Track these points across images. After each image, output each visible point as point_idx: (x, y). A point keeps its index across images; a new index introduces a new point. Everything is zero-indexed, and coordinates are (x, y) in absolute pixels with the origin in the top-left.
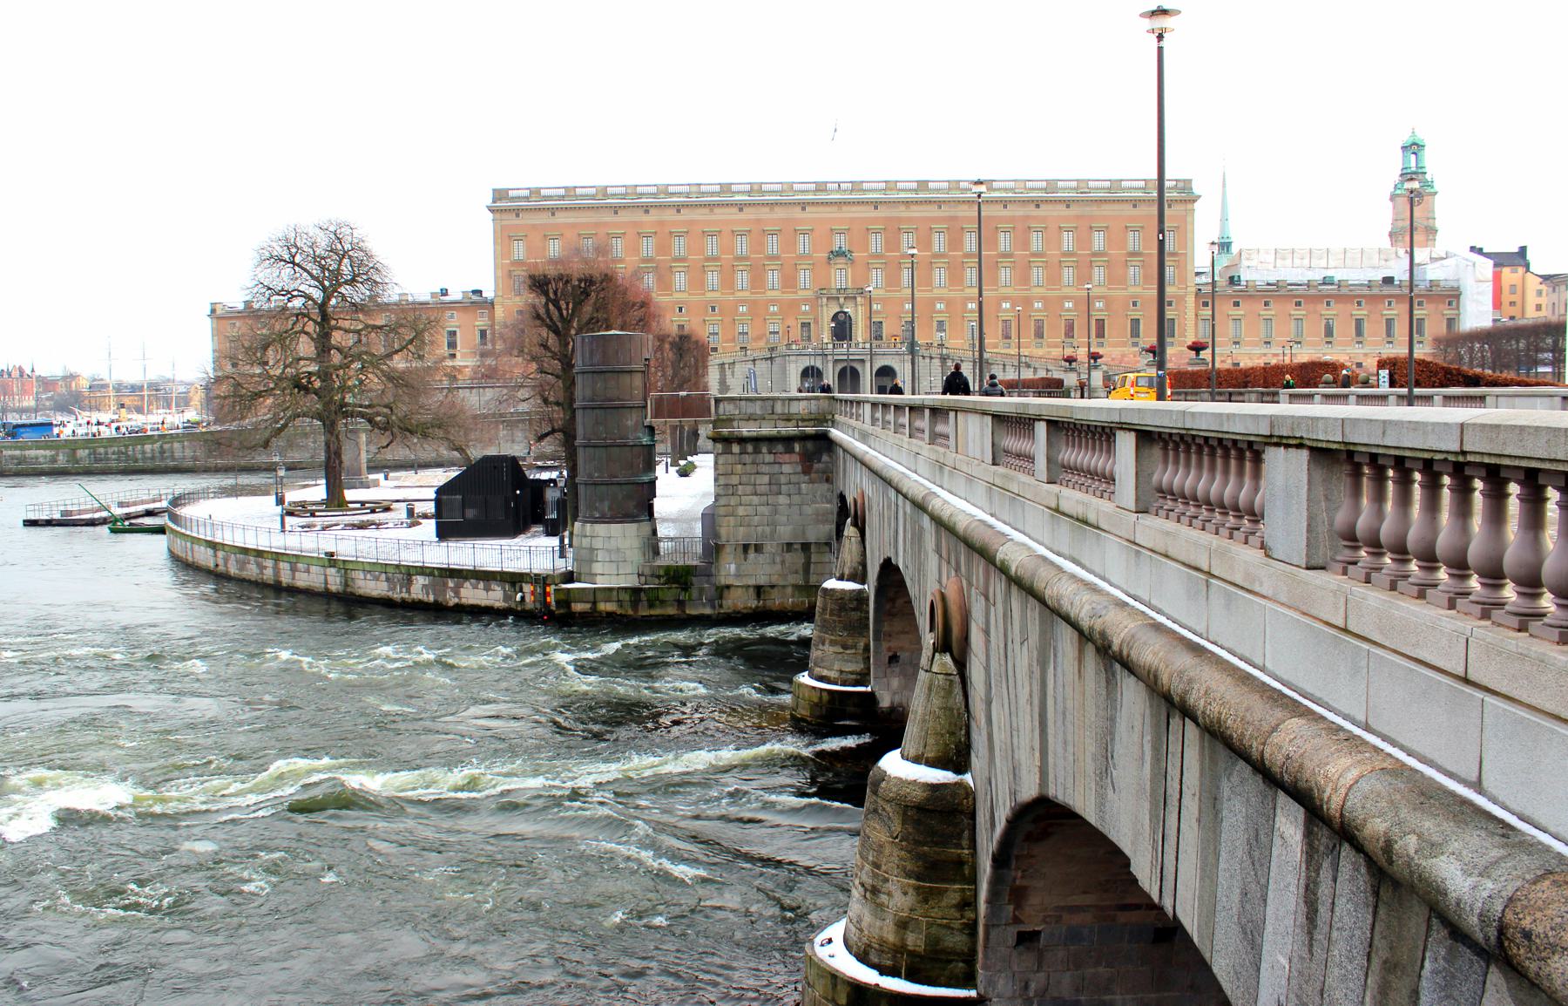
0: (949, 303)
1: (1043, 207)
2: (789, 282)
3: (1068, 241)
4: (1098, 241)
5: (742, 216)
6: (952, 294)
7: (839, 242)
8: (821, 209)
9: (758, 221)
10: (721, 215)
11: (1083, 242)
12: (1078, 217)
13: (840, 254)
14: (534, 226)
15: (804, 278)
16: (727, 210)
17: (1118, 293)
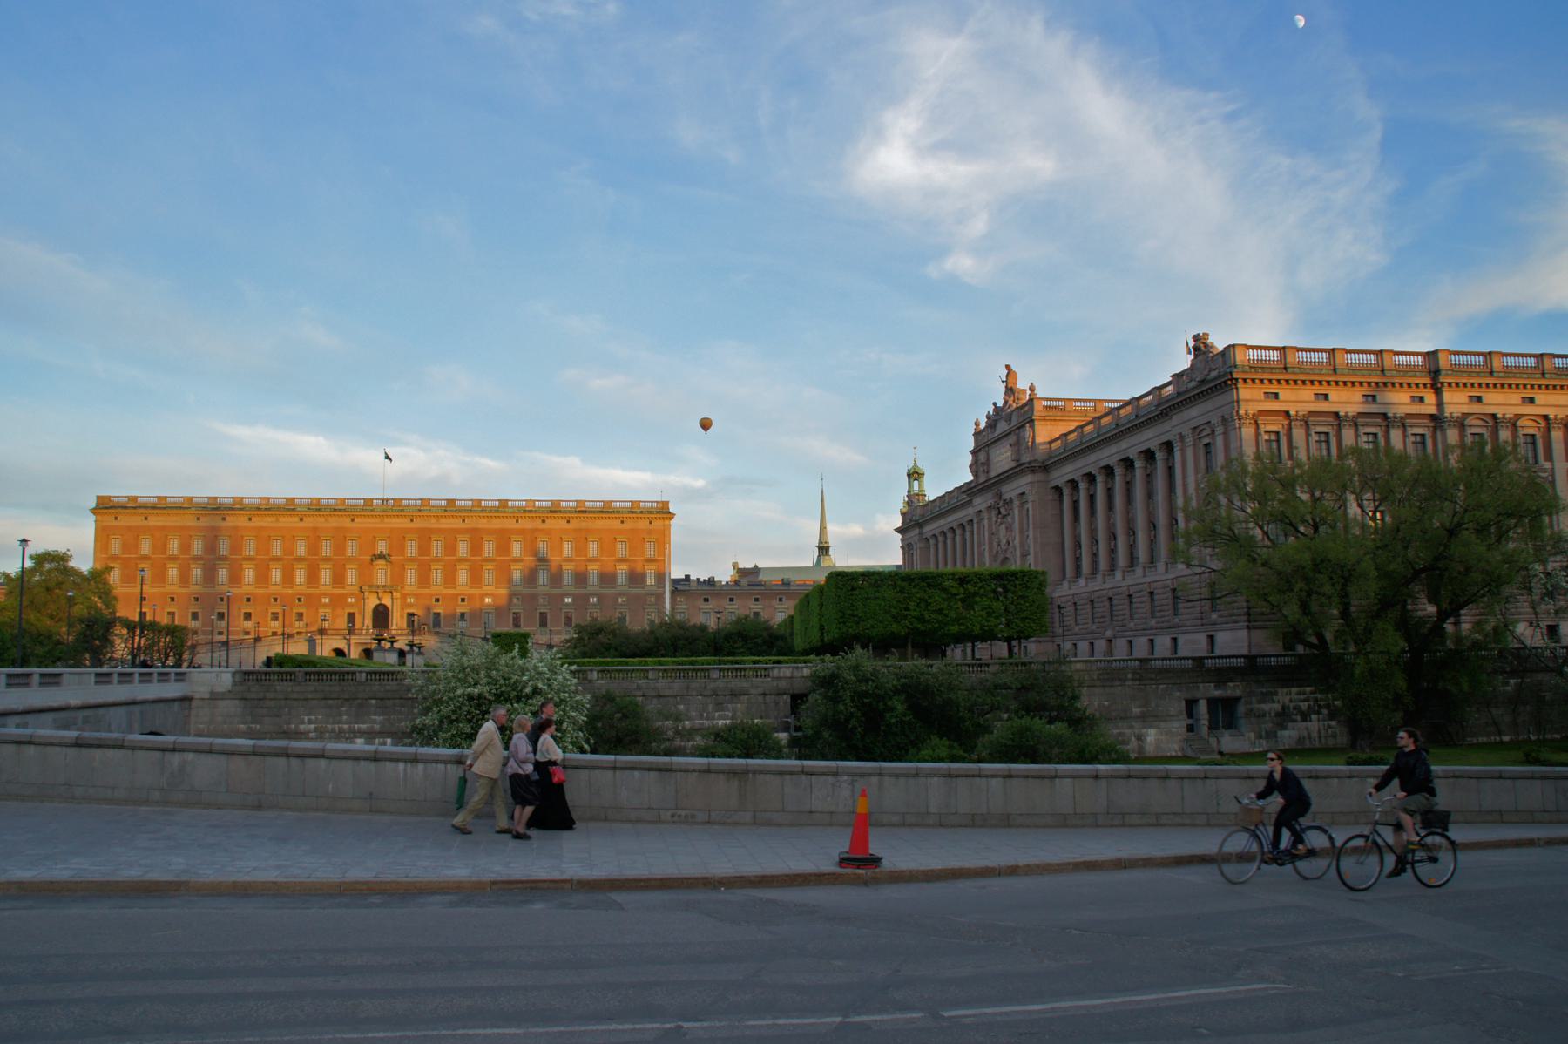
7: (382, 547)
12: (575, 530)
13: (381, 557)
15: (352, 576)
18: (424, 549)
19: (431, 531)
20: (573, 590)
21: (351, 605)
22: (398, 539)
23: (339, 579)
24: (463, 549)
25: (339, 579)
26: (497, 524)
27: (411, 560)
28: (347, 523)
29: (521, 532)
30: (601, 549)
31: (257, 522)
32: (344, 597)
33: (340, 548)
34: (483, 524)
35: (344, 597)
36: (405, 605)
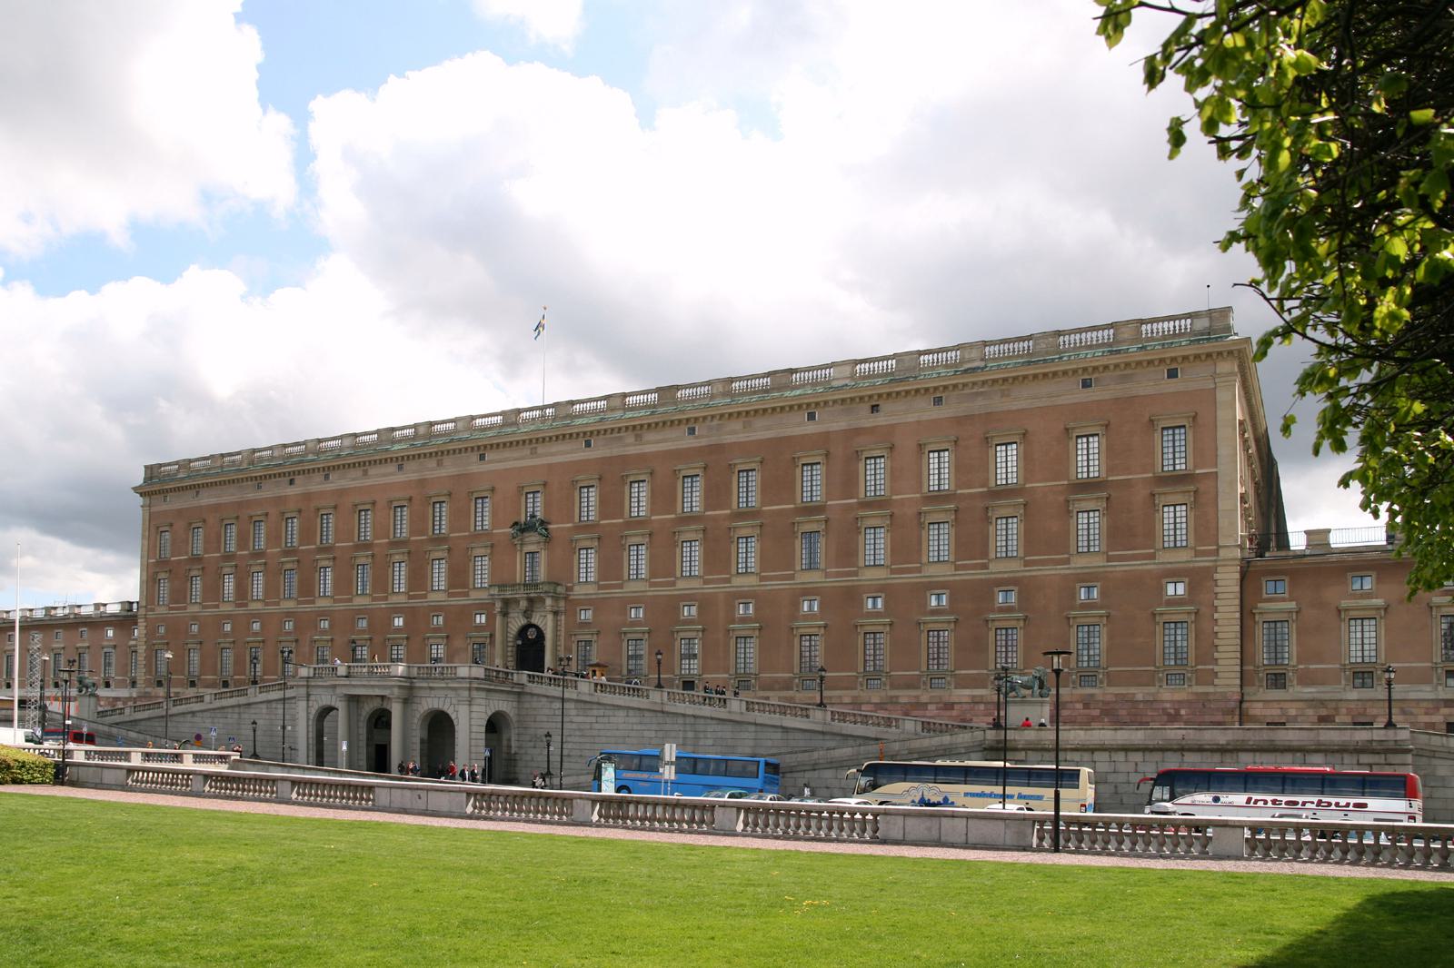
0: (705, 603)
1: (886, 406)
2: (459, 579)
3: (939, 471)
4: (1007, 464)
6: (710, 589)
7: (537, 506)
8: (507, 453)
11: (972, 466)
12: (958, 421)
14: (180, 512)
15: (482, 573)
19: (624, 460)
20: (943, 573)
24: (693, 498)
26: (763, 431)
28: (475, 467)
29: (824, 440)
31: (337, 482)
32: (466, 613)
34: (734, 434)
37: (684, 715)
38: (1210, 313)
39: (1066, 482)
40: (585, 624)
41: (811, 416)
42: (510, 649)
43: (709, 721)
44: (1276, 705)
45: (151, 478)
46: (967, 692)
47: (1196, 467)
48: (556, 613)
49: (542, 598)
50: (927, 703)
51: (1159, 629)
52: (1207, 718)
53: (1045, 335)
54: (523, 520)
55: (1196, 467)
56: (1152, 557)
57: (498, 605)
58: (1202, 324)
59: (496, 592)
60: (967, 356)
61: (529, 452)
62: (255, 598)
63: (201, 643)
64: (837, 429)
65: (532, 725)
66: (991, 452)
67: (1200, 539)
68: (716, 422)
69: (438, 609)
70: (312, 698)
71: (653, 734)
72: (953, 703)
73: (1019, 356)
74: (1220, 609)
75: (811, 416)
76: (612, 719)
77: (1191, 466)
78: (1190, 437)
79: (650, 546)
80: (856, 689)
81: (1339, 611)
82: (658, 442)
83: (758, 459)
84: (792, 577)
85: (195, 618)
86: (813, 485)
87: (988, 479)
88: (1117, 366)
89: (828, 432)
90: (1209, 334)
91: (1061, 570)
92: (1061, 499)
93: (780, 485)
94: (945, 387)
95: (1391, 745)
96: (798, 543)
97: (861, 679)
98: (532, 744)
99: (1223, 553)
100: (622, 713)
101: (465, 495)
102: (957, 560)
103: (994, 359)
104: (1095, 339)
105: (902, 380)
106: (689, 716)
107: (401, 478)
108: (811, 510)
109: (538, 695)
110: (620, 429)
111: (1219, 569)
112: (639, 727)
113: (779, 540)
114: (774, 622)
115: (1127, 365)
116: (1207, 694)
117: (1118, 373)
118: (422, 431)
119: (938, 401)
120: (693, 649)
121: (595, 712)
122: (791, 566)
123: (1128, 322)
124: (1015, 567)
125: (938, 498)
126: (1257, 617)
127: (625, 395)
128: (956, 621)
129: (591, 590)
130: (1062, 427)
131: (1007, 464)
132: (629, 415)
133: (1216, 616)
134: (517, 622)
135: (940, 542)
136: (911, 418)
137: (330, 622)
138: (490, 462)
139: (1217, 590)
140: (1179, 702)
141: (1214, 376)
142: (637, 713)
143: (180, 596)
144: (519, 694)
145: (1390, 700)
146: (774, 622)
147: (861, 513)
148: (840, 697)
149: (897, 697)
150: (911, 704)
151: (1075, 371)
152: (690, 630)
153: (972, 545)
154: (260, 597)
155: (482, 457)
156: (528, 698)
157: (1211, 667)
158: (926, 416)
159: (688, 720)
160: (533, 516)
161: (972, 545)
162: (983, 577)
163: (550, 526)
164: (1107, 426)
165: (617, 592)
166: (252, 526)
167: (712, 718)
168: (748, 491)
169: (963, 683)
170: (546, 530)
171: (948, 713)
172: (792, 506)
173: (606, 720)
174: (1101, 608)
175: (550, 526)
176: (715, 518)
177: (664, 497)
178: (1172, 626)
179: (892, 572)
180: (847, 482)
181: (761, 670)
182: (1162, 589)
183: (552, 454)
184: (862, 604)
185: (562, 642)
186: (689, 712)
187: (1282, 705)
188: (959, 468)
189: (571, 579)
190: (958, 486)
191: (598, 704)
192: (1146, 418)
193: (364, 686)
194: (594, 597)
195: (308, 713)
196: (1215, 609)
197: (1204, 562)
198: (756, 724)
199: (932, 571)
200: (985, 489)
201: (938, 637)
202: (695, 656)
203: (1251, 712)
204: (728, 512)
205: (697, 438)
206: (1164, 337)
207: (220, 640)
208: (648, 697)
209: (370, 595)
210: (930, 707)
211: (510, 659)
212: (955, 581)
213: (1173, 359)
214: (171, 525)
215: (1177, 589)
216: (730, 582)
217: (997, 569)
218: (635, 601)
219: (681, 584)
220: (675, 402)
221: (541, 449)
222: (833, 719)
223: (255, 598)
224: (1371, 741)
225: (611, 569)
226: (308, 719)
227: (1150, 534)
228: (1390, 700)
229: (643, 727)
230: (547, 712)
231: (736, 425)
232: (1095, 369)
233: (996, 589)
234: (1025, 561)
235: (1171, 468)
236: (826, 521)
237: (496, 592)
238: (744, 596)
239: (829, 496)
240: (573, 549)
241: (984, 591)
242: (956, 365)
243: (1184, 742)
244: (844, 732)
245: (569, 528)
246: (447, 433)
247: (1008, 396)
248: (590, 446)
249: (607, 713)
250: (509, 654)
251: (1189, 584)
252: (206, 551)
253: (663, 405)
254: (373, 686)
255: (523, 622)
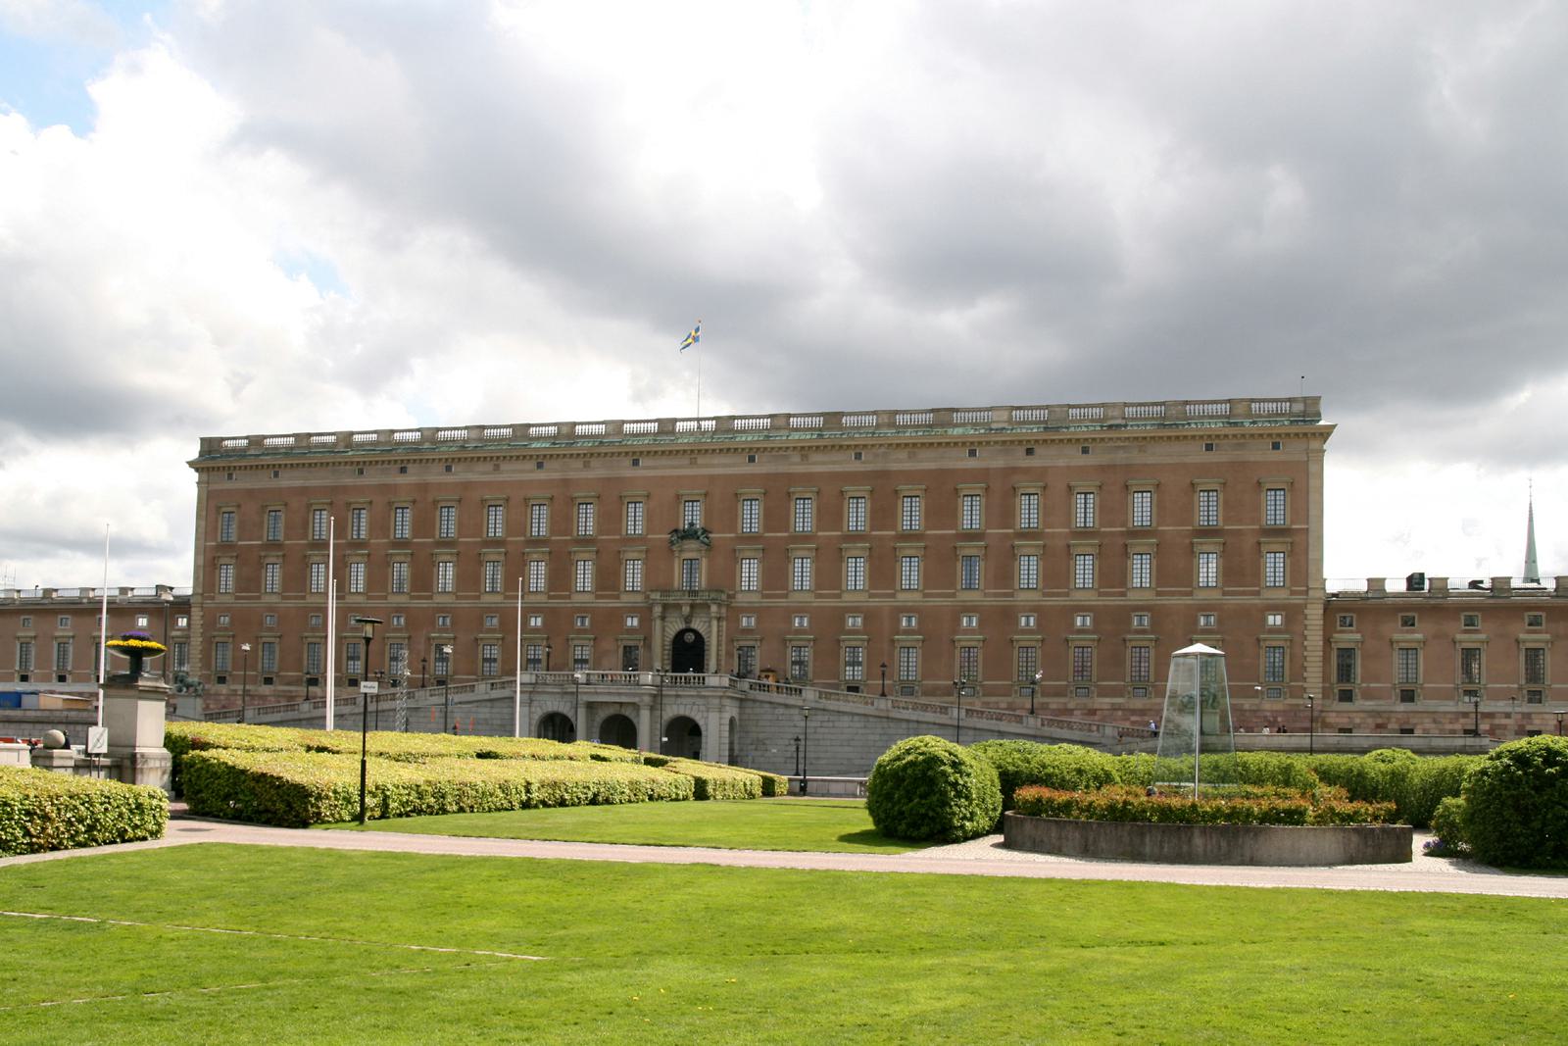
0: (870, 615)
3: (1085, 512)
4: (1142, 509)
5: (541, 475)
6: (875, 602)
7: (694, 515)
8: (664, 461)
9: (566, 482)
10: (511, 473)
11: (1113, 508)
12: (1103, 469)
13: (690, 534)
14: (250, 493)
15: (634, 576)
16: (519, 466)
17: (1174, 601)
18: (776, 517)
19: (791, 478)
20: (1092, 599)
21: (632, 630)
22: (726, 498)
23: (608, 579)
24: (857, 516)
25: (608, 579)
26: (927, 462)
27: (751, 539)
28: (626, 471)
29: (983, 475)
30: (1160, 509)
31: (460, 475)
32: (616, 616)
33: (611, 518)
34: (900, 462)
35: (616, 616)
36: (734, 634)
37: (908, 721)
38: (1305, 400)
39: (1191, 528)
40: (747, 631)
41: (972, 453)
42: (666, 652)
43: (931, 726)
44: (1346, 715)
45: (210, 452)
46: (1107, 700)
47: (1292, 522)
48: (719, 619)
49: (707, 604)
50: (1073, 710)
51: (1262, 652)
52: (1298, 725)
53: (1176, 403)
54: (681, 528)
55: (1292, 522)
56: (1258, 593)
57: (658, 610)
58: (1298, 407)
59: (658, 597)
60: (1110, 414)
61: (582, 466)
62: (353, 590)
63: (280, 637)
64: (995, 466)
65: (754, 729)
66: (1130, 497)
67: (1294, 582)
68: (883, 450)
69: (583, 611)
70: (535, 703)
71: (877, 737)
72: (1096, 710)
73: (1153, 418)
74: (1308, 638)
75: (972, 453)
76: (836, 724)
77: (1288, 522)
78: (1288, 499)
79: (646, 562)
80: (1010, 696)
81: (1455, 643)
82: (824, 463)
83: (924, 487)
84: (953, 595)
85: (271, 609)
86: (971, 515)
87: (1127, 520)
88: (1235, 436)
89: (988, 469)
90: (1304, 416)
91: (1187, 601)
92: (1187, 541)
93: (942, 509)
94: (1094, 439)
95: (1478, 749)
96: (959, 565)
97: (1016, 688)
98: (753, 747)
99: (1311, 593)
100: (846, 718)
101: (473, 503)
102: (1100, 587)
103: (1133, 419)
104: (1215, 411)
105: (1054, 427)
106: (913, 721)
107: (541, 475)
108: (971, 536)
109: (762, 702)
110: (787, 448)
111: (1308, 606)
112: (863, 731)
113: (942, 562)
114: (937, 634)
115: (1243, 436)
116: (1298, 705)
117: (1235, 441)
118: (565, 430)
119: (1085, 451)
120: (858, 657)
121: (820, 718)
122: (952, 585)
123: (1242, 400)
124: (1148, 597)
125: (1085, 533)
126: (1333, 645)
127: (789, 416)
128: (1099, 640)
129: (755, 598)
130: (1188, 481)
131: (1142, 509)
132: (796, 436)
133: (1306, 643)
134: (675, 626)
135: (1084, 571)
136: (1061, 463)
137: (1152, 618)
138: (644, 468)
139: (1307, 622)
140: (1276, 711)
141: (1307, 451)
142: (863, 719)
143: (250, 583)
144: (741, 700)
145: (1476, 712)
146: (937, 634)
147: (959, 544)
148: (997, 703)
149: (1047, 704)
150: (1059, 710)
151: (1201, 437)
152: (855, 640)
153: (1113, 575)
154: (449, 588)
155: (636, 463)
156: (750, 704)
157: (1300, 684)
158: (960, 465)
159: (911, 725)
160: (692, 524)
161: (1113, 575)
162: (1122, 603)
163: (710, 535)
164: (1225, 484)
165: (782, 602)
166: (350, 514)
167: (935, 724)
168: (911, 515)
169: (1104, 692)
170: (708, 538)
171: (1092, 718)
172: (839, 533)
173: (831, 724)
174: (1217, 633)
175: (710, 535)
176: (881, 538)
177: (831, 514)
178: (1272, 650)
179: (1044, 595)
180: (1004, 513)
181: (925, 677)
182: (1265, 620)
183: (713, 466)
184: (1017, 622)
185: (724, 647)
186: (914, 718)
187: (1351, 715)
188: (1104, 510)
189: (733, 586)
190: (1101, 526)
191: (824, 710)
192: (1256, 479)
193: (609, 693)
194: (756, 605)
195: (530, 719)
196: (1305, 638)
197: (1297, 600)
198: (975, 729)
199: (1078, 596)
200: (1124, 529)
201: (969, 652)
202: (859, 664)
203: (1328, 720)
204: (893, 533)
205: (864, 463)
206: (1269, 416)
207: (306, 634)
208: (872, 704)
209: (454, 594)
210: (1075, 712)
211: (666, 662)
212: (1098, 605)
213: (1279, 435)
214: (239, 506)
215: (1275, 620)
216: (840, 597)
217: (1133, 598)
218: (800, 611)
219: (846, 597)
220: (840, 427)
221: (701, 460)
222: (1043, 725)
223: (353, 590)
224: (1465, 746)
225: (776, 577)
226: (530, 724)
227: (1257, 574)
228: (1476, 712)
229: (868, 731)
230: (769, 717)
231: (903, 454)
232: (1218, 436)
233: (1133, 614)
234: (1291, 591)
235: (1140, 524)
236: (986, 547)
237: (658, 597)
238: (908, 610)
239: (988, 525)
240: (734, 559)
241: (1123, 615)
242: (1099, 420)
243: (1339, 746)
244: (1054, 736)
245: (730, 538)
246: (501, 440)
247: (1145, 452)
248: (754, 461)
249: (832, 718)
250: (666, 657)
251: (1286, 616)
252: (287, 537)
253: (829, 429)
254: (619, 694)
255: (681, 626)
